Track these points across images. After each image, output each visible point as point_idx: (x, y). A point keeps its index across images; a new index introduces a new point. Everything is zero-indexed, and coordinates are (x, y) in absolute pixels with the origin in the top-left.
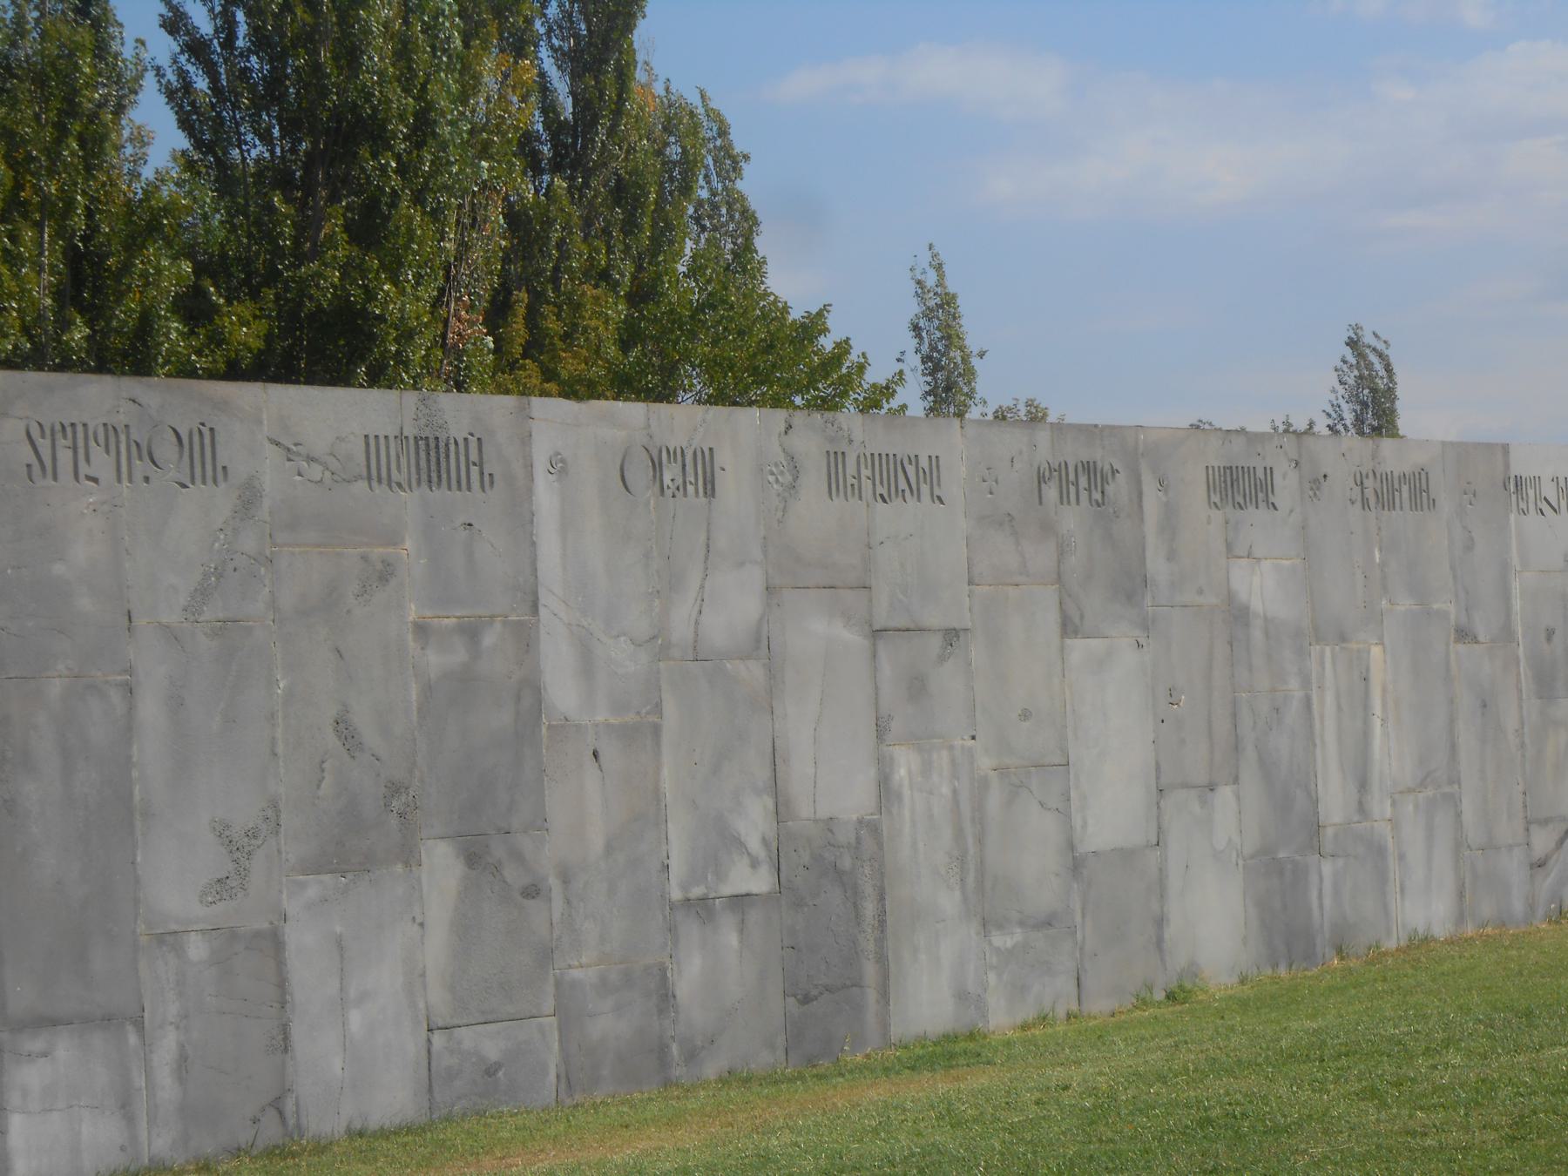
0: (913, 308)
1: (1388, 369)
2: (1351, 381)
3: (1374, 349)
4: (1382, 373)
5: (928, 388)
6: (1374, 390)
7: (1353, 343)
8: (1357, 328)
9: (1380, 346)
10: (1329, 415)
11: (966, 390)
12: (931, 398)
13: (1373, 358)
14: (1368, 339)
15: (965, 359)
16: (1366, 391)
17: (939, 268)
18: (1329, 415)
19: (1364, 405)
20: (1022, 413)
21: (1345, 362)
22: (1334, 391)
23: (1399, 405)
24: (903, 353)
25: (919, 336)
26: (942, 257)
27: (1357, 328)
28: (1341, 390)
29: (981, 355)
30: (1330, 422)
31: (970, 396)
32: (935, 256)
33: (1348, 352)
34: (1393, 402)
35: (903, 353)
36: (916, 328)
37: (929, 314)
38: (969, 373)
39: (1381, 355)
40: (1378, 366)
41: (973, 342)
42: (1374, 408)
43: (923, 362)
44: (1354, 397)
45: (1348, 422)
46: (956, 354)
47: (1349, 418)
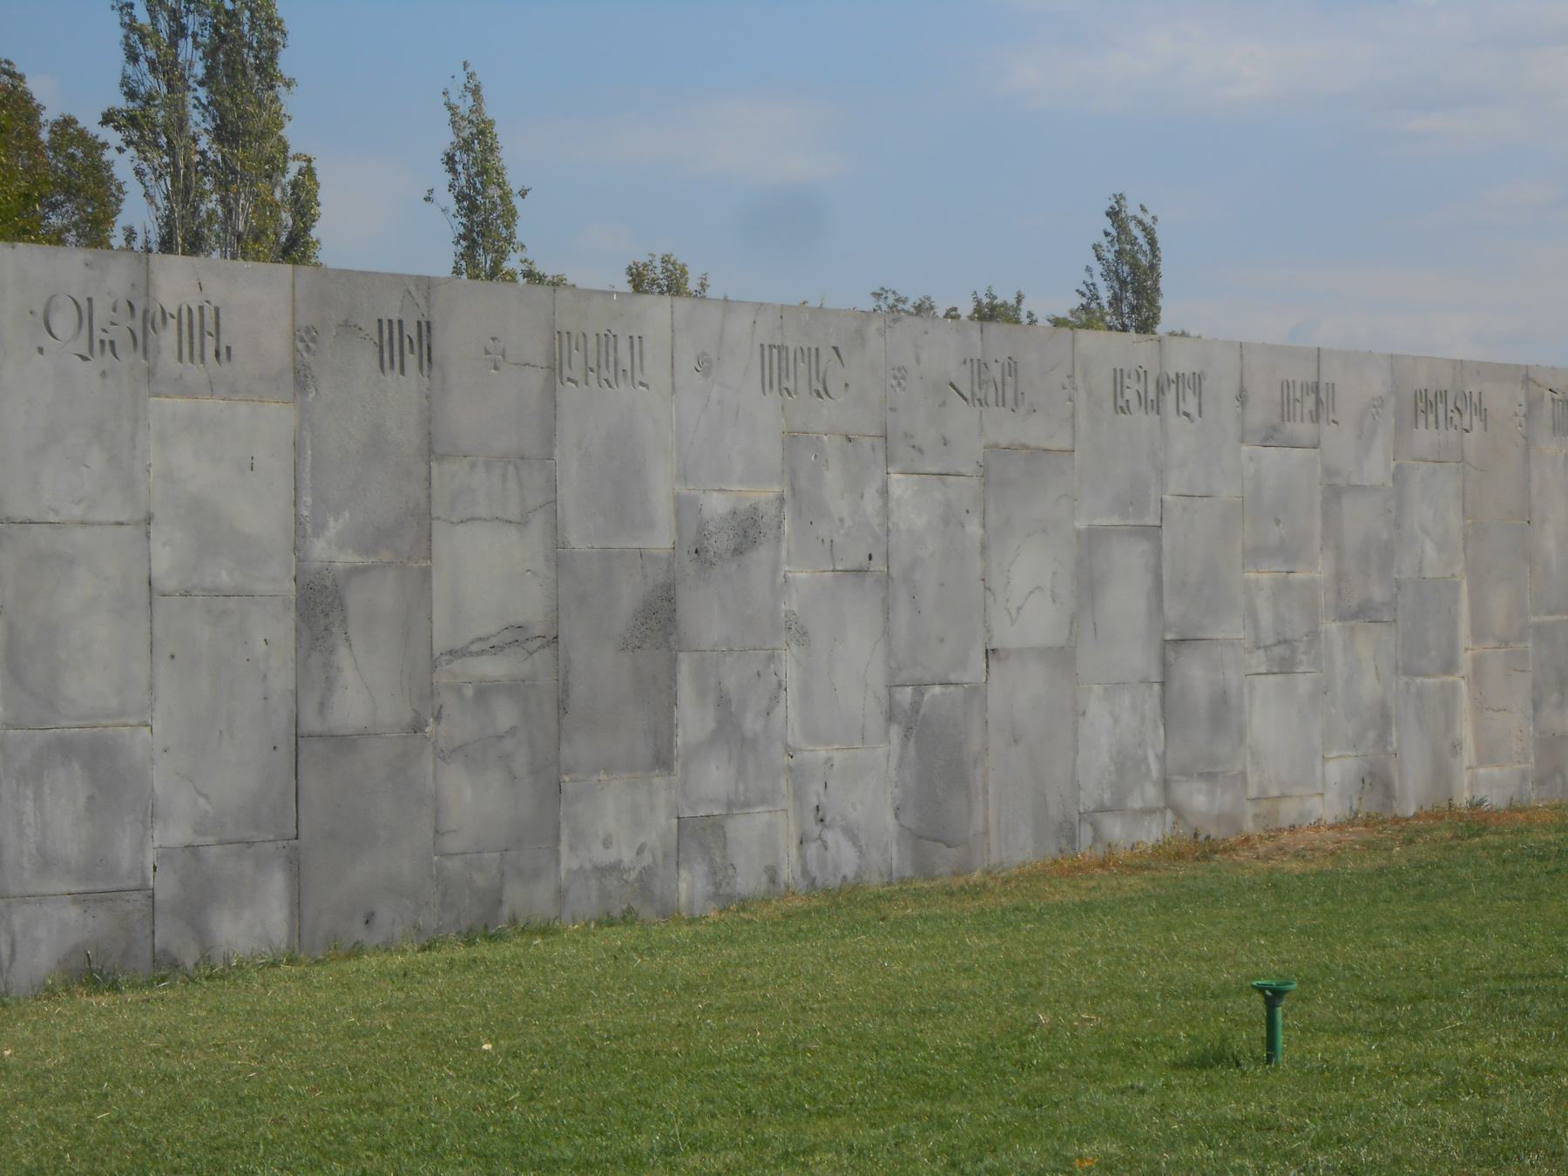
0: (446, 139)
1: (1152, 242)
2: (1111, 256)
3: (1140, 222)
4: (1146, 247)
5: (462, 230)
6: (1135, 266)
7: (1113, 214)
8: (1120, 199)
9: (1147, 220)
10: (1083, 295)
11: (504, 233)
12: (464, 243)
13: (1137, 232)
14: (1131, 209)
15: (505, 197)
16: (1126, 268)
17: (476, 92)
18: (1083, 295)
19: (1123, 283)
20: (658, 271)
21: (1107, 234)
22: (1088, 269)
23: (1162, 284)
24: (431, 191)
25: (453, 170)
26: (479, 78)
27: (1120, 199)
28: (1098, 268)
29: (523, 194)
30: (1084, 301)
31: (509, 240)
32: (471, 76)
33: (1108, 221)
34: (1156, 281)
35: (431, 191)
36: (450, 160)
37: (466, 146)
38: (510, 215)
39: (1144, 230)
40: (1142, 240)
41: (514, 181)
42: (1131, 288)
43: (458, 201)
44: (1112, 274)
45: (1105, 302)
46: (494, 192)
47: (1105, 295)
